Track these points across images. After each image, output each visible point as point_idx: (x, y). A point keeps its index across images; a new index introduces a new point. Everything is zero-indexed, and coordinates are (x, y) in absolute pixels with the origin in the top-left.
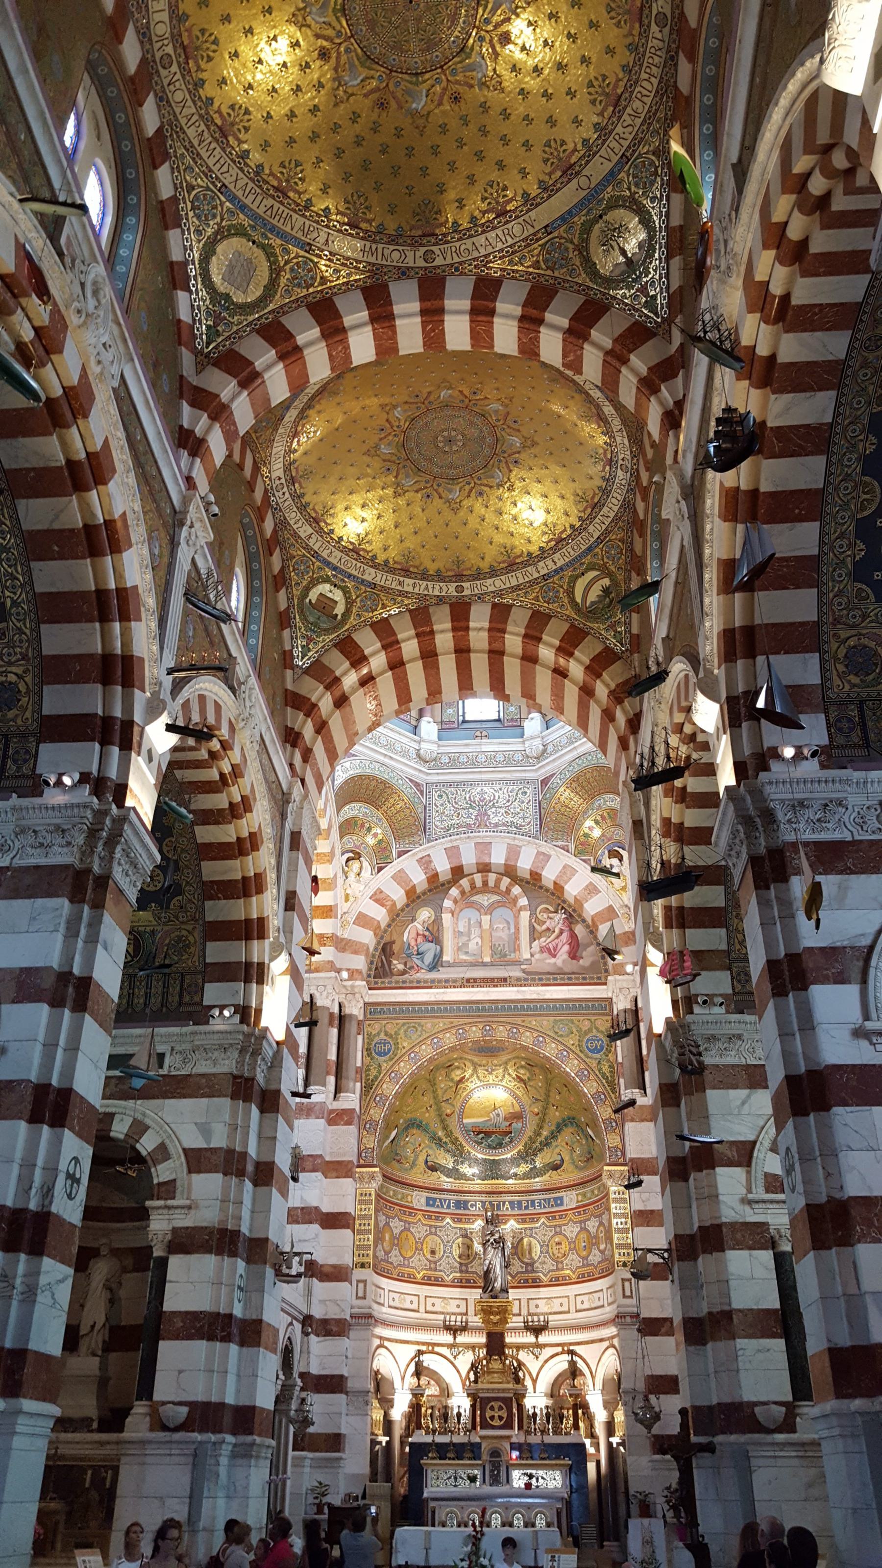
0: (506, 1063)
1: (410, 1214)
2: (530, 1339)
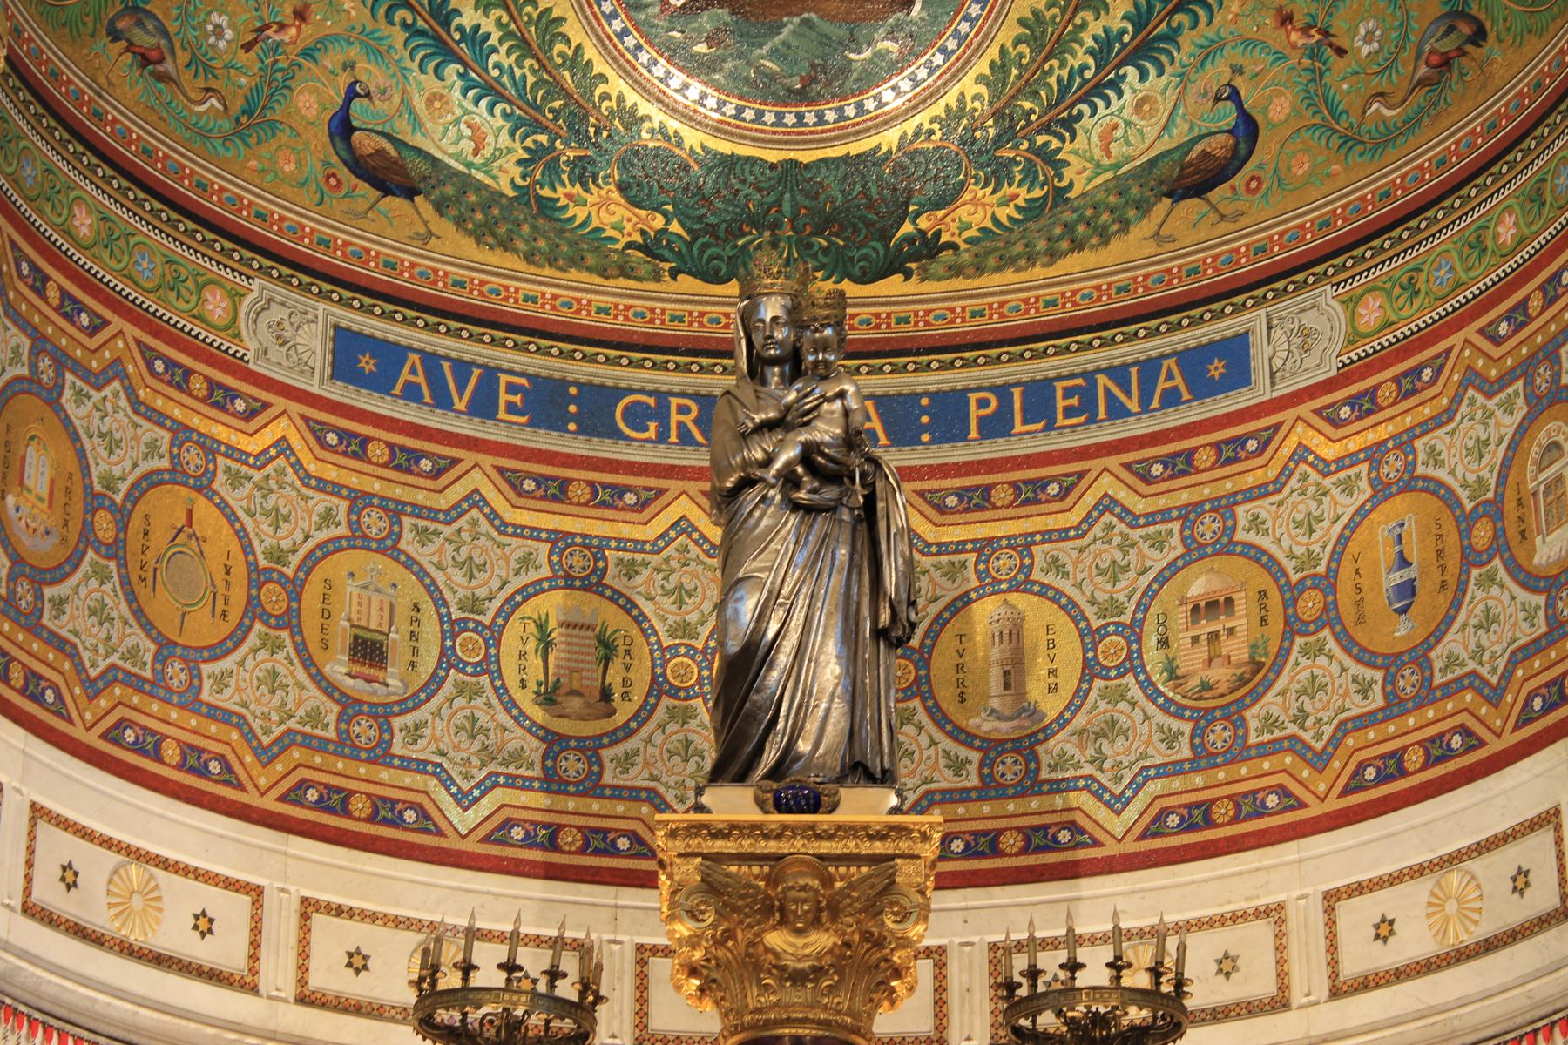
1: (219, 398)
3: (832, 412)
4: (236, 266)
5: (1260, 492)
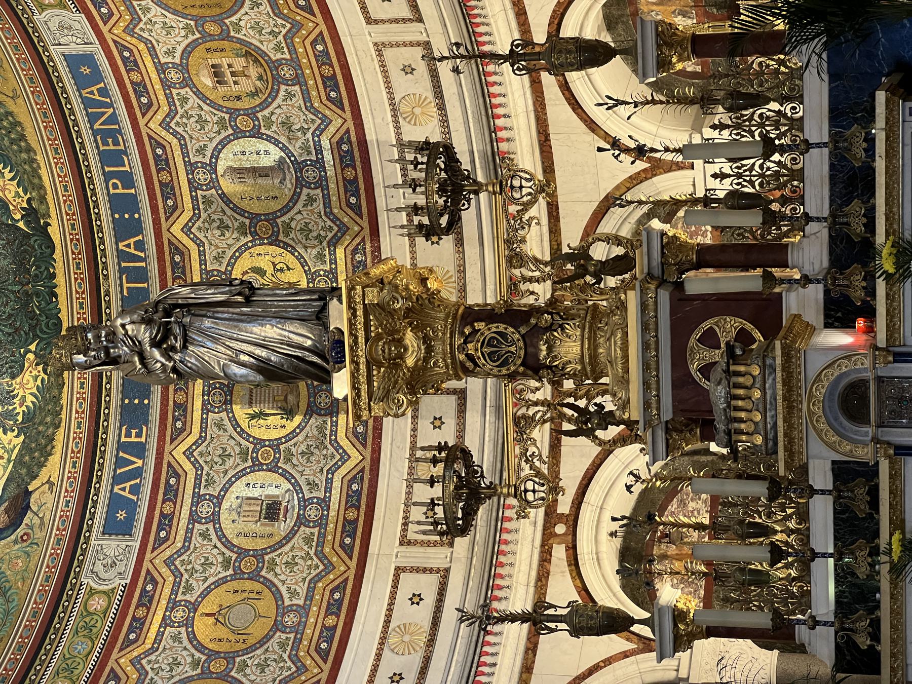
1: (147, 601)
3: (133, 330)
4: (75, 593)
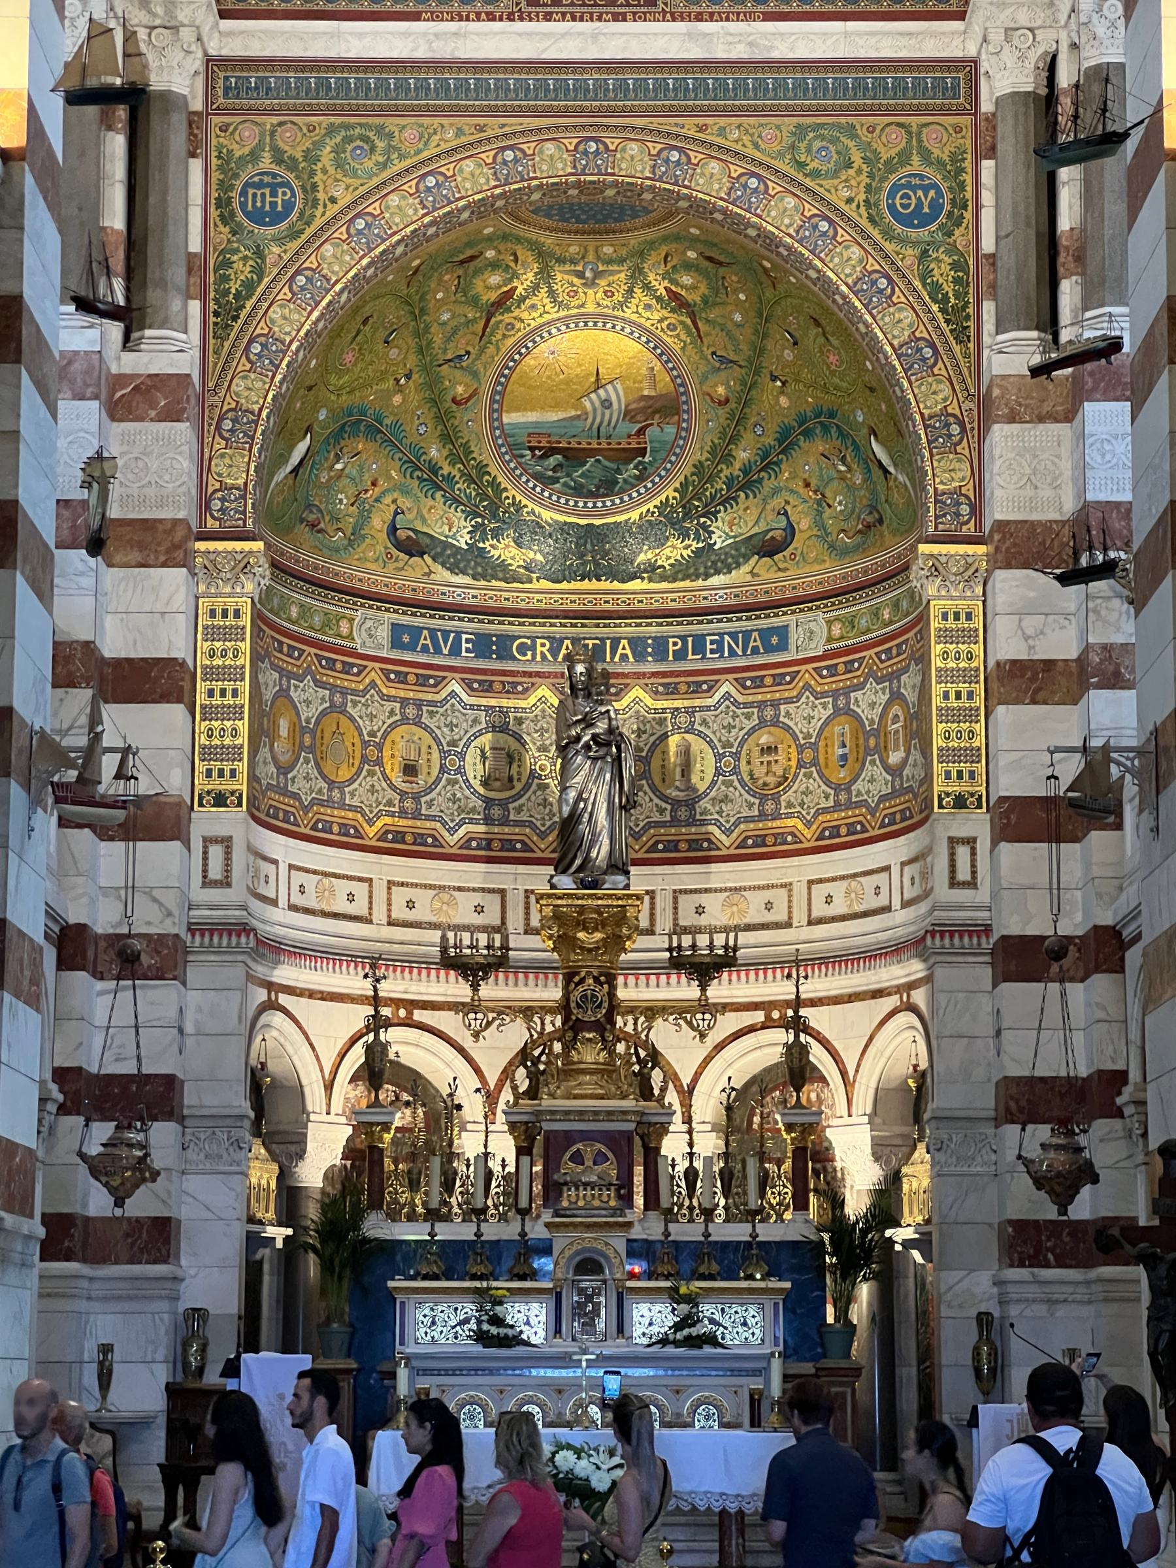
0: (641, 254)
1: (347, 669)
2: (685, 990)
5: (789, 701)
